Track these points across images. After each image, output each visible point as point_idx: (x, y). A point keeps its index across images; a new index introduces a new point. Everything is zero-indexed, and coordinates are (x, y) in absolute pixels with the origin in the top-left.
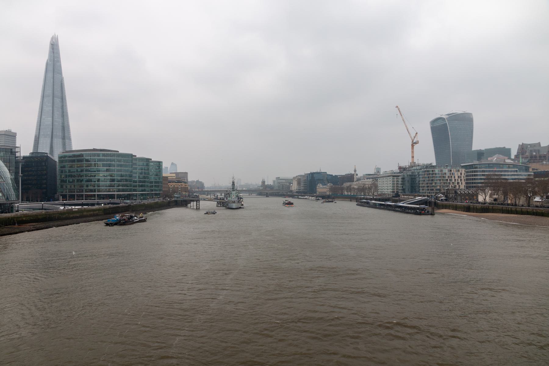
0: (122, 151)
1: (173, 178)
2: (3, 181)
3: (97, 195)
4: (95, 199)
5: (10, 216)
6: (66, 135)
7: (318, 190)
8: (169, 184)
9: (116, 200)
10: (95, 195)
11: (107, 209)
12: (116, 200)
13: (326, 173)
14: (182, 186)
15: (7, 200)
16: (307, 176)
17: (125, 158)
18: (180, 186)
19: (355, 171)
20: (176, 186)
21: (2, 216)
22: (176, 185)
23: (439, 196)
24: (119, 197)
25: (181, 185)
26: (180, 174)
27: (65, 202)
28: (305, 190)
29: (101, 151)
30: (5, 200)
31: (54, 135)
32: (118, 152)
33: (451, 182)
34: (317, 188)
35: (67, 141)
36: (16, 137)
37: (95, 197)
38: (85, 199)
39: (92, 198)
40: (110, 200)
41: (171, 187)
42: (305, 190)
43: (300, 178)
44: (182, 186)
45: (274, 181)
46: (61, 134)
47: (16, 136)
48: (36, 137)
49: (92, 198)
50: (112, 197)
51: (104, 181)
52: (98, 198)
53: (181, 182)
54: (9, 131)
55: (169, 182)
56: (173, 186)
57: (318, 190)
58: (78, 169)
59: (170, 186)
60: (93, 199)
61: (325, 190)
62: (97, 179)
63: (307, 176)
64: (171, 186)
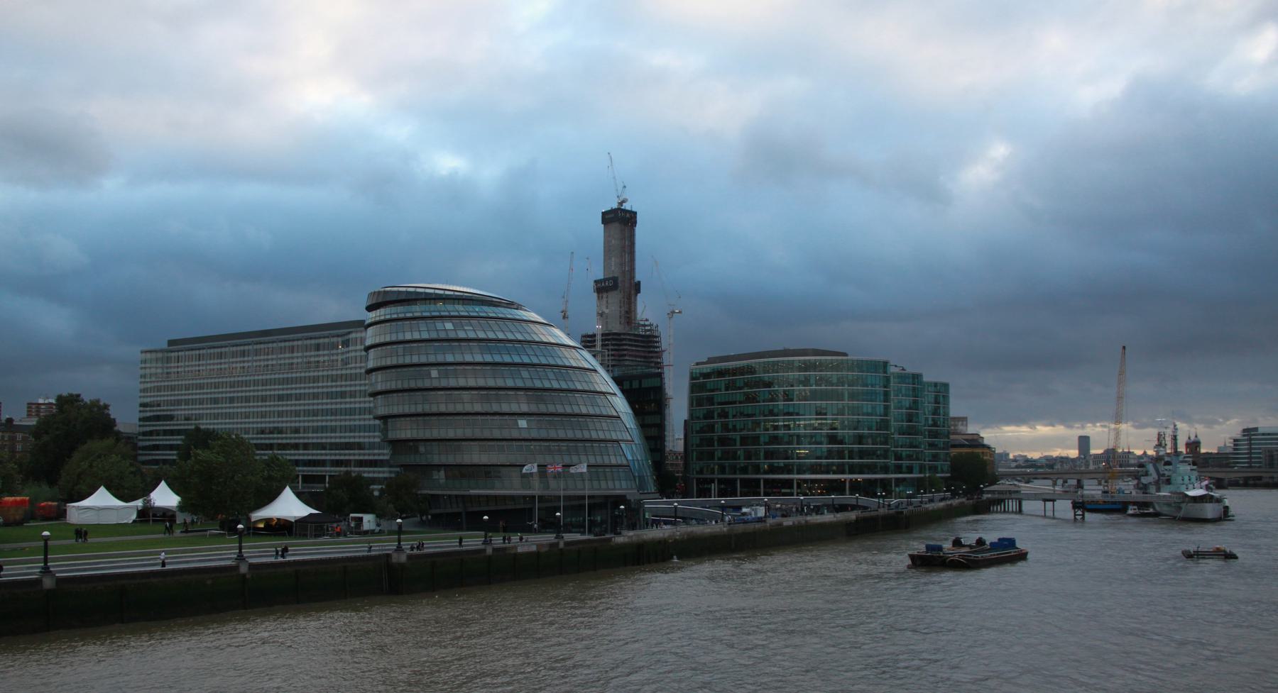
3: (798, 479)
4: (792, 494)
5: (661, 535)
10: (792, 480)
11: (851, 523)
12: (848, 498)
15: (641, 492)
21: (646, 535)
24: (856, 487)
27: (802, 498)
30: (636, 491)
32: (845, 354)
37: (791, 487)
39: (783, 491)
40: (857, 498)
45: (1235, 440)
49: (783, 491)
50: (837, 487)
51: (813, 439)
52: (799, 491)
58: (731, 409)
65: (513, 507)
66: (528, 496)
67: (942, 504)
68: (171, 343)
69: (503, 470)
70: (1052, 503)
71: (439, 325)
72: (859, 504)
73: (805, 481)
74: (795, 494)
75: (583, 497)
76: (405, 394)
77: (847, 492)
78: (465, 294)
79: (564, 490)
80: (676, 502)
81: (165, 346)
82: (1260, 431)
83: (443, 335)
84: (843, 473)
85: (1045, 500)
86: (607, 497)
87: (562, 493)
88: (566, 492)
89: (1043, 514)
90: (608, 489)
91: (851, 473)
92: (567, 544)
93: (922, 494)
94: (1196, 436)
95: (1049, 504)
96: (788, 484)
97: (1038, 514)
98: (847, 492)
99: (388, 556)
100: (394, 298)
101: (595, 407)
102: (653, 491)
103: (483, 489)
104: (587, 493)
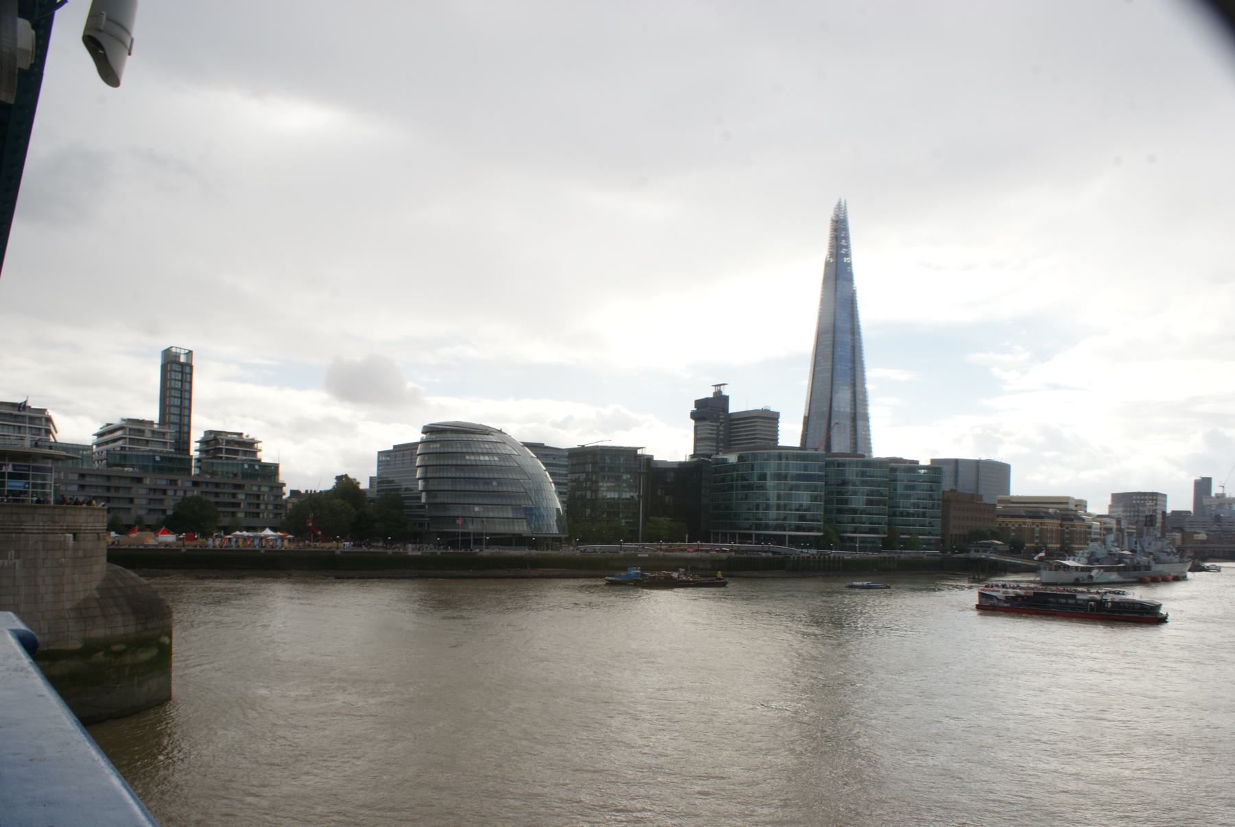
1: (1027, 505)
2: (530, 502)
3: (756, 534)
6: (859, 410)
8: (1000, 519)
9: (786, 548)
10: (752, 534)
12: (786, 548)
14: (1043, 527)
17: (818, 461)
18: (1037, 526)
20: (1023, 526)
22: (1025, 523)
24: (794, 541)
25: (1041, 524)
26: (1134, 497)
31: (833, 414)
35: (859, 423)
36: (779, 420)
37: (752, 540)
38: (755, 544)
41: (1013, 528)
44: (1043, 527)
46: (848, 410)
47: (779, 417)
48: (805, 417)
53: (1042, 517)
54: (766, 411)
55: (998, 516)
56: (1017, 526)
59: (1010, 526)
60: (749, 543)
62: (755, 504)
64: (1013, 525)
67: (876, 555)
68: (395, 447)
72: (771, 550)
73: (761, 534)
74: (754, 542)
75: (482, 534)
81: (391, 448)
86: (514, 534)
92: (442, 553)
93: (901, 549)
96: (749, 537)
102: (557, 532)
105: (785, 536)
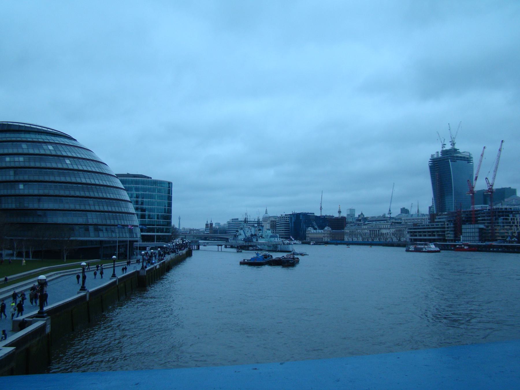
0: (155, 177)
7: (309, 235)
13: (314, 214)
16: (291, 218)
19: (340, 212)
23: (513, 240)
28: (285, 235)
29: (135, 177)
32: (151, 178)
33: (514, 225)
34: (307, 232)
42: (285, 235)
43: (273, 220)
57: (309, 235)
61: (321, 236)
63: (291, 218)
65: (90, 246)
66: (112, 241)
69: (77, 227)
70: (221, 246)
71: (45, 146)
76: (9, 184)
77: (155, 241)
78: (54, 131)
79: (118, 237)
80: (169, 244)
82: (239, 220)
83: (48, 152)
84: (154, 232)
85: (218, 245)
87: (118, 239)
88: (119, 239)
89: (218, 250)
90: (123, 237)
91: (157, 232)
94: (211, 221)
95: (220, 247)
97: (216, 250)
98: (155, 241)
99: (138, 272)
100: (6, 128)
101: (114, 195)
103: (82, 237)
104: (129, 239)
105: (154, 235)
